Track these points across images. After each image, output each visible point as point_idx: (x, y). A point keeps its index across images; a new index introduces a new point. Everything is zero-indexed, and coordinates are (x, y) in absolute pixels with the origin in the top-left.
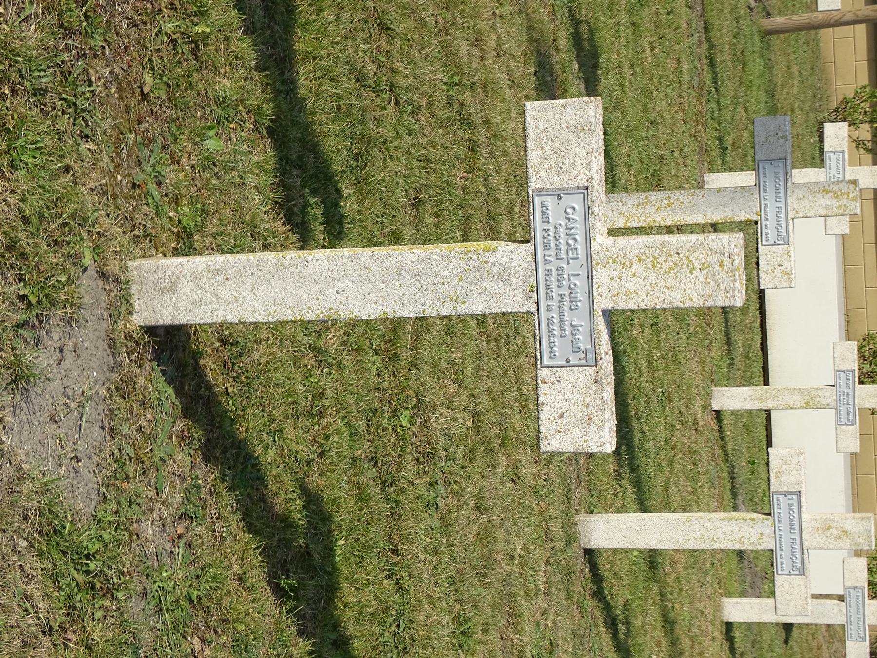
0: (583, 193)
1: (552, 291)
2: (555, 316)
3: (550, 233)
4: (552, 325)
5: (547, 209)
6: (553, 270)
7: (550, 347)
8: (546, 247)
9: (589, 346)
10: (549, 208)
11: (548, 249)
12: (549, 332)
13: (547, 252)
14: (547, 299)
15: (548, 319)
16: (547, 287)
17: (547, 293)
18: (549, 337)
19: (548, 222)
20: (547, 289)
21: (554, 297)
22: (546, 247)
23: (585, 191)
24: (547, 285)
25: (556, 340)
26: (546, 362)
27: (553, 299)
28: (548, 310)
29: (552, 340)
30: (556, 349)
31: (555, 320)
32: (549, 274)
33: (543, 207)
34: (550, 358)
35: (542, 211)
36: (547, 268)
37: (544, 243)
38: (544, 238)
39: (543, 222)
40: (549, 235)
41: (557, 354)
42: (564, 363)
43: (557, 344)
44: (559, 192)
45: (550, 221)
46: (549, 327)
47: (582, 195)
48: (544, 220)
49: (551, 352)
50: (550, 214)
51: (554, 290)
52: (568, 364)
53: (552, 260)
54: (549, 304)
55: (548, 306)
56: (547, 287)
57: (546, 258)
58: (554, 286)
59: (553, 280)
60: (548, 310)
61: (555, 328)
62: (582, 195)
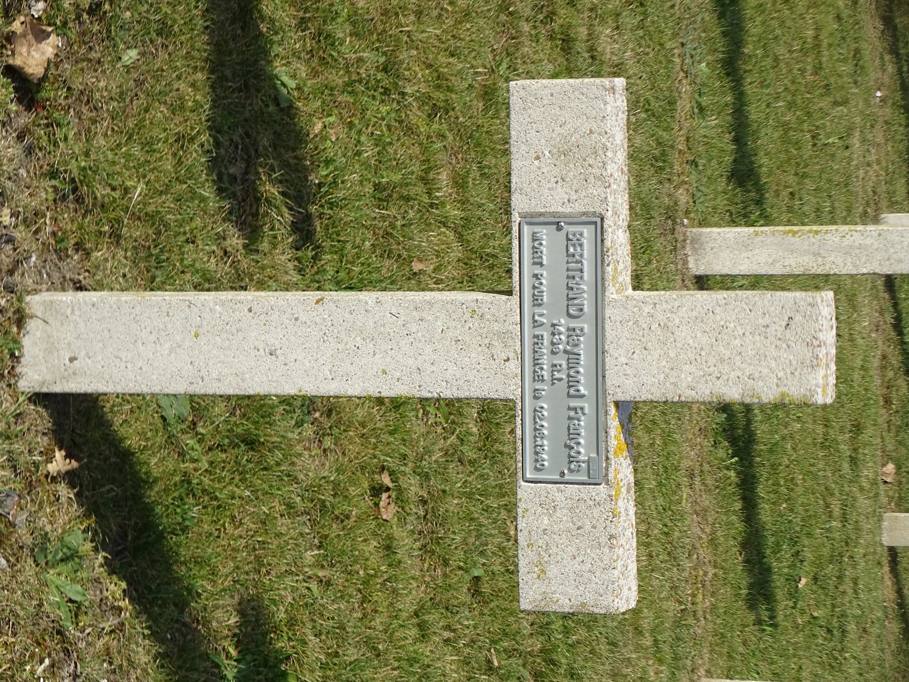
0: (595, 223)
1: (542, 369)
2: (545, 406)
3: (544, 282)
4: (541, 420)
5: (541, 244)
6: (545, 337)
7: (537, 453)
8: (537, 301)
9: (594, 455)
10: (544, 242)
11: (540, 305)
12: (536, 429)
13: (538, 310)
14: (534, 380)
15: (535, 410)
16: (536, 363)
17: (535, 372)
18: (535, 437)
19: (541, 264)
20: (535, 365)
21: (546, 378)
22: (537, 301)
23: (598, 220)
24: (535, 359)
25: (545, 442)
26: (528, 476)
27: (543, 380)
28: (536, 398)
29: (539, 443)
30: (545, 456)
31: (545, 413)
32: (540, 341)
33: (534, 240)
34: (536, 469)
35: (534, 247)
36: (536, 333)
37: (534, 295)
38: (534, 287)
39: (534, 263)
40: (541, 284)
41: (546, 463)
42: (557, 477)
43: (546, 448)
44: (558, 220)
45: (545, 262)
46: (536, 423)
47: (593, 227)
48: (536, 260)
49: (536, 461)
50: (545, 252)
51: (545, 367)
52: (562, 480)
53: (545, 321)
54: (537, 387)
55: (536, 390)
56: (536, 363)
57: (537, 318)
58: (545, 361)
59: (545, 351)
60: (536, 398)
61: (545, 424)
62: (593, 227)
